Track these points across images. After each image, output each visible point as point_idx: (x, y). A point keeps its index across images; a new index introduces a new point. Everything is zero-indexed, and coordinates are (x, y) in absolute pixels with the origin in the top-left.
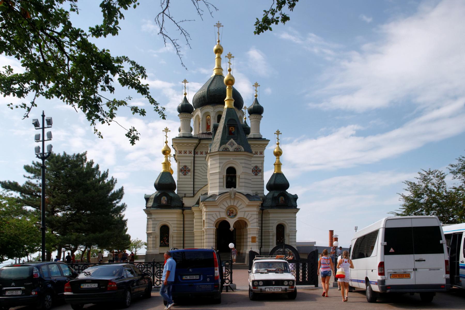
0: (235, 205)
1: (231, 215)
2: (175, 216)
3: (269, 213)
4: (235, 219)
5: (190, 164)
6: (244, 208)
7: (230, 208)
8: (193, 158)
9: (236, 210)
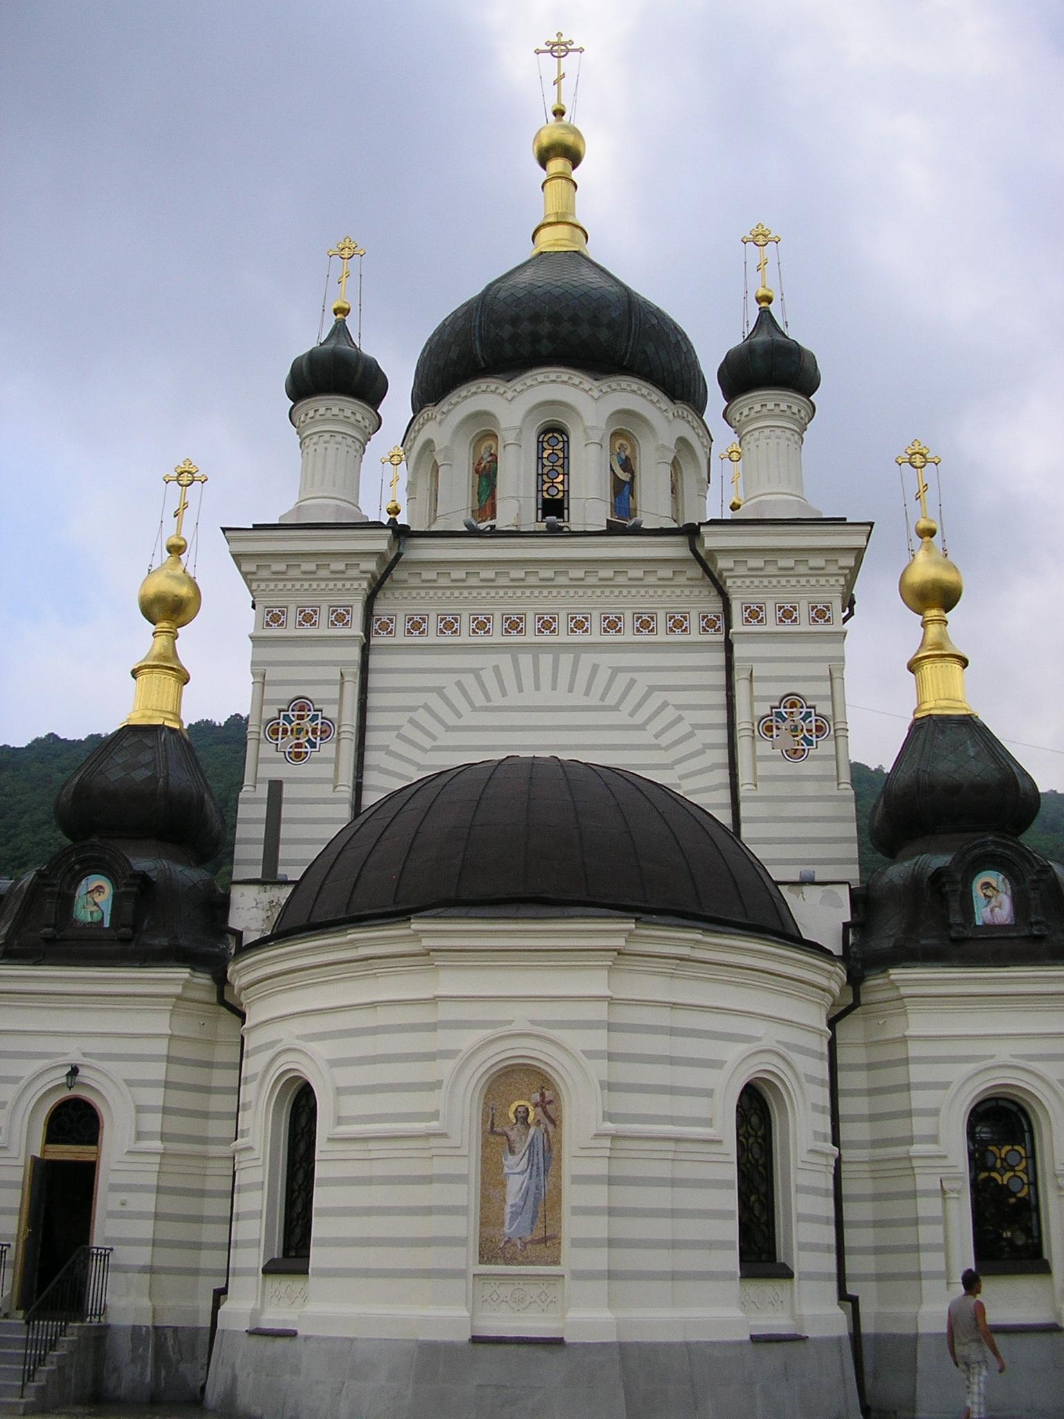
2: (160, 1022)
5: (334, 692)
8: (355, 654)
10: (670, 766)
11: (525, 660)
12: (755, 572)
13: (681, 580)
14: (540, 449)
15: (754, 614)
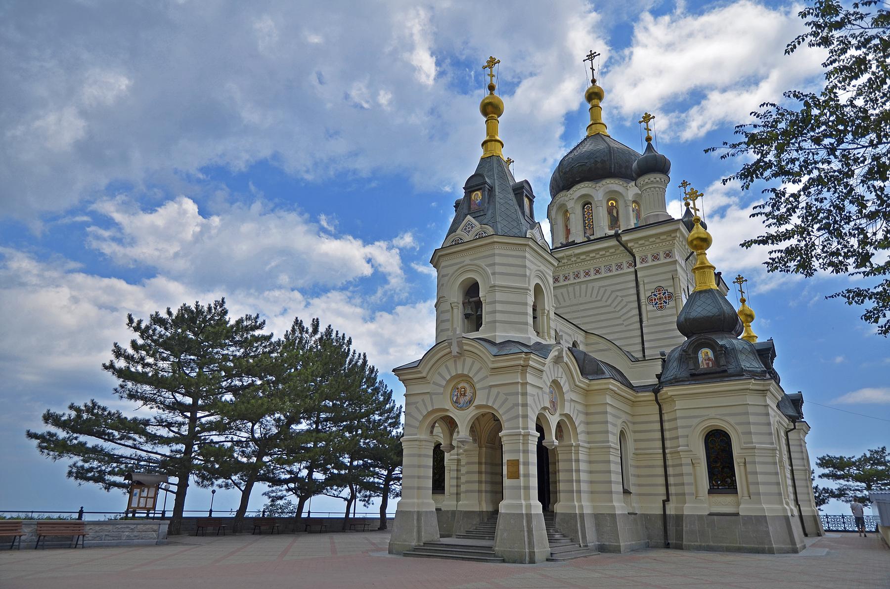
0: (466, 372)
1: (462, 400)
3: (672, 399)
4: (471, 413)
6: (486, 377)
7: (458, 383)
9: (473, 386)
10: (619, 318)
11: (571, 289)
12: (642, 245)
13: (618, 252)
14: (584, 212)
15: (643, 260)
